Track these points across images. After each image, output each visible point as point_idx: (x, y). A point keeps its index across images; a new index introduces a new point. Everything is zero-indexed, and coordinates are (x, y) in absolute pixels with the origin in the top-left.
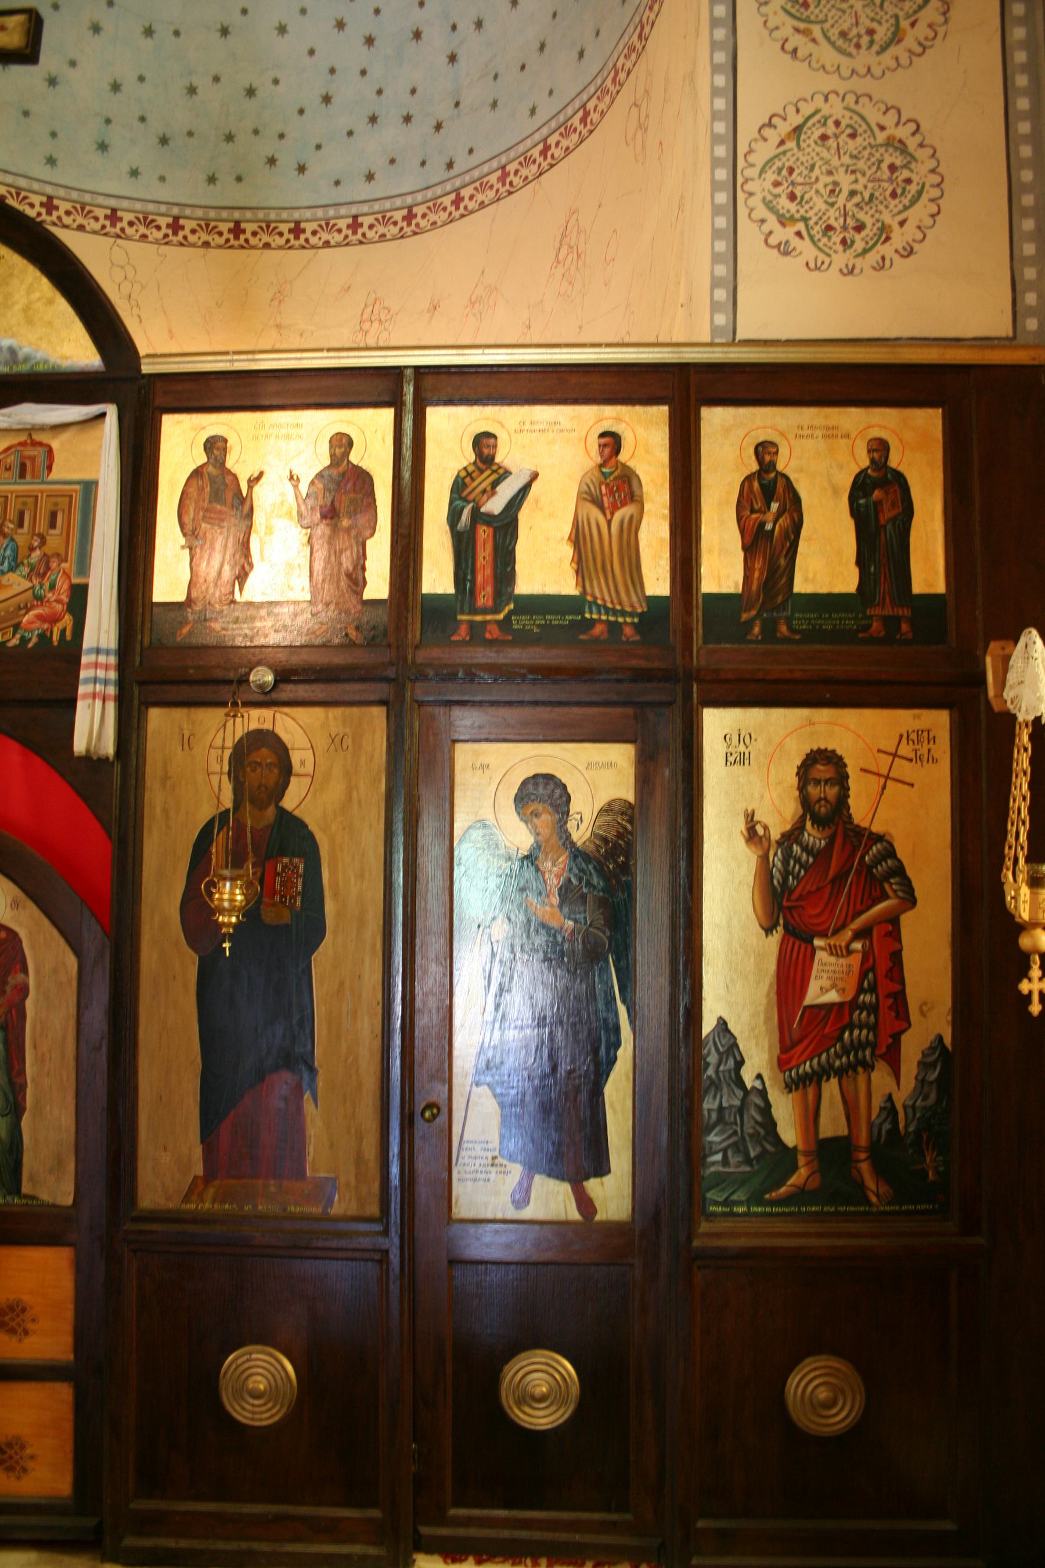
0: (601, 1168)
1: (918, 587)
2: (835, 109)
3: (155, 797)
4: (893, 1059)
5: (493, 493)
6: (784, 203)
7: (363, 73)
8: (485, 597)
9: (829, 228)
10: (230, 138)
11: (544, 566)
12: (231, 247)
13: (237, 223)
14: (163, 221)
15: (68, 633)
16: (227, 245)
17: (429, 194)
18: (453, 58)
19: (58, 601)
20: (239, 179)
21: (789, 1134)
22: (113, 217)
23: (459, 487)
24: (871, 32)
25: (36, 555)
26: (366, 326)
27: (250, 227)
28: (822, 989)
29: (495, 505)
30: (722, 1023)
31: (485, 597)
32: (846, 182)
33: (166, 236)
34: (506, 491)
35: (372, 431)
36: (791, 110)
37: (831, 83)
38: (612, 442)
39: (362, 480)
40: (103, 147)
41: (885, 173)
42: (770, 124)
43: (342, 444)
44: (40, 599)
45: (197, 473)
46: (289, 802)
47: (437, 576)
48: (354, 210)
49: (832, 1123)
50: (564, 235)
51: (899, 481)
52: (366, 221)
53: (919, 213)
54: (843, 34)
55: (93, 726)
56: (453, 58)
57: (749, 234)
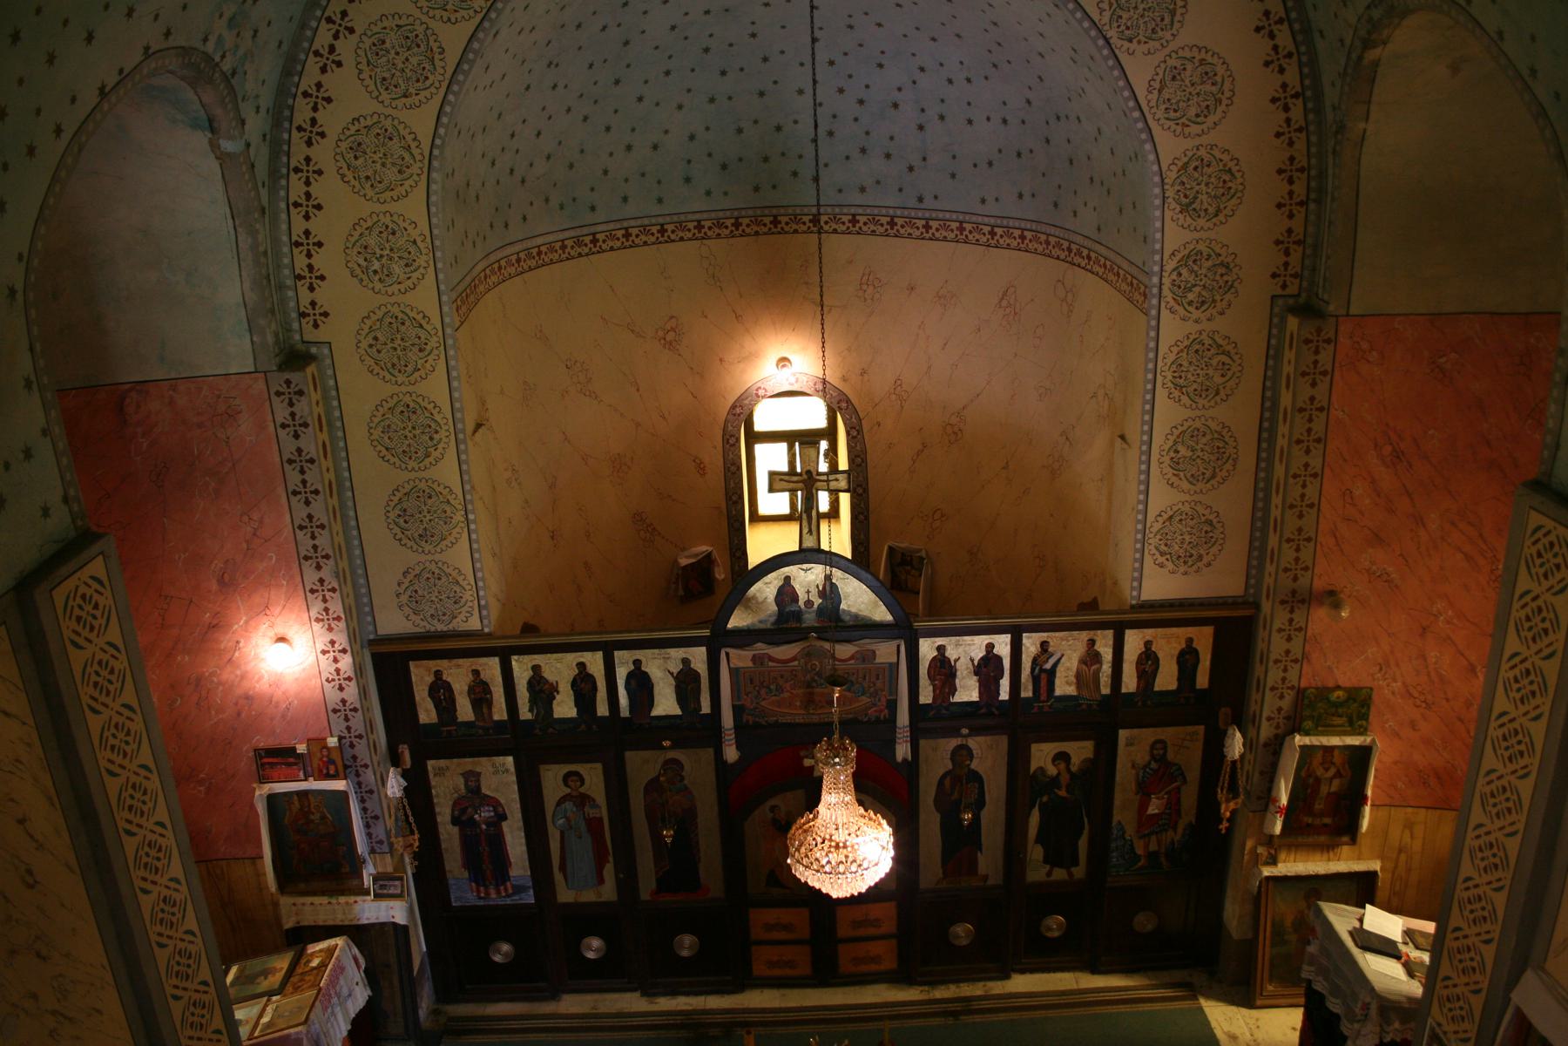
0: (1077, 864)
1: (1198, 687)
2: (1186, 508)
3: (923, 768)
4: (1175, 828)
6: (1163, 548)
7: (856, 119)
10: (766, 159)
11: (1064, 686)
14: (729, 222)
17: (906, 213)
18: (921, 128)
20: (774, 187)
21: (1140, 851)
22: (699, 227)
23: (1035, 661)
27: (784, 219)
28: (1152, 810)
29: (1048, 666)
32: (1187, 538)
34: (1052, 661)
37: (1187, 497)
38: (1092, 642)
39: (999, 659)
43: (990, 647)
47: (1027, 692)
48: (853, 211)
49: (1153, 847)
50: (1005, 294)
52: (862, 219)
53: (1214, 550)
55: (902, 751)
56: (921, 128)
57: (1148, 559)
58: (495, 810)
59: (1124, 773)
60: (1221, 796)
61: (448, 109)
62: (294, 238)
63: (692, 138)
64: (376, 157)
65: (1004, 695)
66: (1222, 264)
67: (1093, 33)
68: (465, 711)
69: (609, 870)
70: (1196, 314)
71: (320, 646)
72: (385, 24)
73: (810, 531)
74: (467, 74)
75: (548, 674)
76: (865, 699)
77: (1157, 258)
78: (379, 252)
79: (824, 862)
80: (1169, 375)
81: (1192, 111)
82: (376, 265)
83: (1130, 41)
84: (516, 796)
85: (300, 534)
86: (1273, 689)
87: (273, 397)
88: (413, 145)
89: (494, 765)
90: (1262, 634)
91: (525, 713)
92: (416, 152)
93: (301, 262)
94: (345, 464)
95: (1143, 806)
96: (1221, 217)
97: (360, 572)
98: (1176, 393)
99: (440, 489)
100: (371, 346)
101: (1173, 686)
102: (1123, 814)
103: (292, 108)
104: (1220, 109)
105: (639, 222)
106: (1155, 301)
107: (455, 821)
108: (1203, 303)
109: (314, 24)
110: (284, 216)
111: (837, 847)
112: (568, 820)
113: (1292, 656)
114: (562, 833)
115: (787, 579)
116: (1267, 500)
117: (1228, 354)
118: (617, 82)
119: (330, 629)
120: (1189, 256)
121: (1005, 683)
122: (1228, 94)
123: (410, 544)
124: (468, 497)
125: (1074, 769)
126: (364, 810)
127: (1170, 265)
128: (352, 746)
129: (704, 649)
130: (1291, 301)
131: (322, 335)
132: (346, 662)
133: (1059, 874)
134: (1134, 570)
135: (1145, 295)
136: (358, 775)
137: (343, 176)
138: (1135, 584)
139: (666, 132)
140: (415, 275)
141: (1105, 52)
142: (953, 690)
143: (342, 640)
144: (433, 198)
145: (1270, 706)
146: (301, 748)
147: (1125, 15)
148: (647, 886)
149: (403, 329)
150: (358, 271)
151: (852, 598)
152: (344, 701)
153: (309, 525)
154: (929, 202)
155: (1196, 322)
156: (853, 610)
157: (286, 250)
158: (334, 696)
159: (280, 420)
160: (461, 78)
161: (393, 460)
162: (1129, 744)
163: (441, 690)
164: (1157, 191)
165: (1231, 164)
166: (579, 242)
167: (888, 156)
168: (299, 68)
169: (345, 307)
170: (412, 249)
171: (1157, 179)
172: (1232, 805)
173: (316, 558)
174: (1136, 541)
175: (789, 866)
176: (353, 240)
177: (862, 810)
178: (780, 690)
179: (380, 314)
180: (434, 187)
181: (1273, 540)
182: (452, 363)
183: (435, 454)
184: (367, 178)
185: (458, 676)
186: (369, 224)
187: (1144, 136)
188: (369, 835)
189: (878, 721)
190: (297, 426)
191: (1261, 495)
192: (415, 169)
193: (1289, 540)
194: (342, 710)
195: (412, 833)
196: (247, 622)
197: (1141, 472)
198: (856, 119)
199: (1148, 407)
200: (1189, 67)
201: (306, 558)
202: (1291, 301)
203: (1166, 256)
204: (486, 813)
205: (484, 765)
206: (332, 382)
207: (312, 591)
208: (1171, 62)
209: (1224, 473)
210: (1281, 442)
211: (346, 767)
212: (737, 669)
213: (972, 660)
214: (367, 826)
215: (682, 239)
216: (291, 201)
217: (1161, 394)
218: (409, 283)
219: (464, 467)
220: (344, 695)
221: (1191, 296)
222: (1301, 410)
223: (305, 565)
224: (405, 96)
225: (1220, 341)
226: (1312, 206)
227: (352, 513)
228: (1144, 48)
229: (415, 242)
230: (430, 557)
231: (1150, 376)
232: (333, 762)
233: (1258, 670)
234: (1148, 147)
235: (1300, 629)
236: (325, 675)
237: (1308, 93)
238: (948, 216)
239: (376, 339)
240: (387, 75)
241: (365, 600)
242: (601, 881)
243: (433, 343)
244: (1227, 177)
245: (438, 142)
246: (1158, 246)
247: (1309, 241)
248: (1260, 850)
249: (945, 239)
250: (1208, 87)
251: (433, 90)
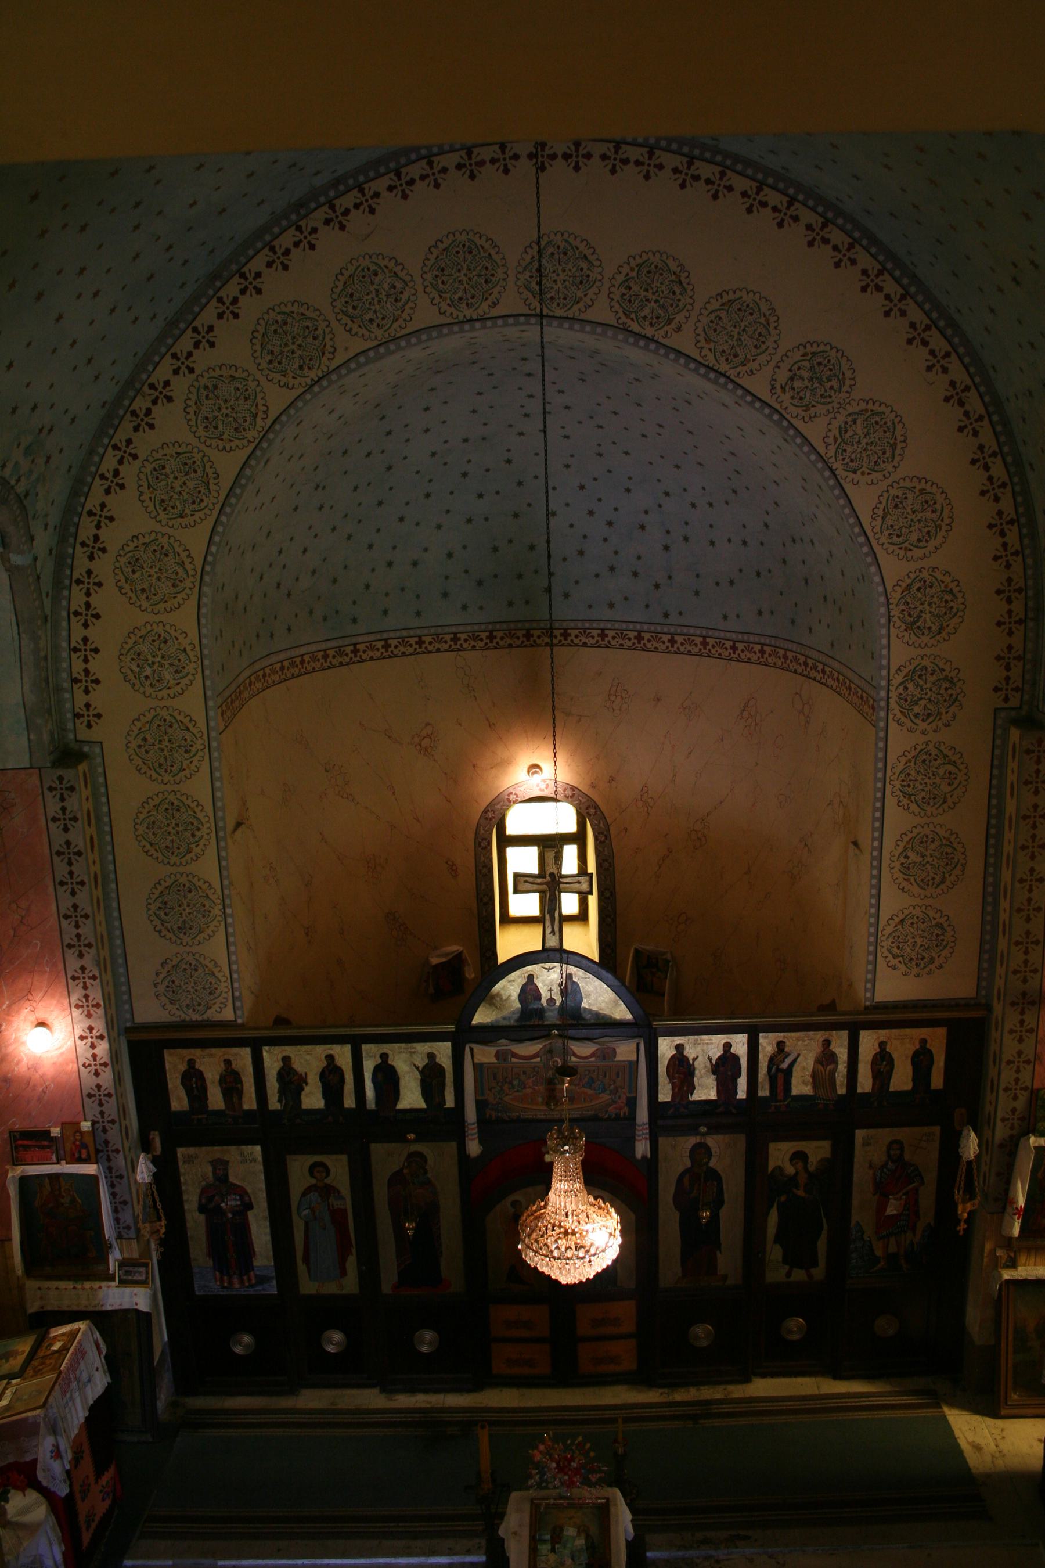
0: (815, 1264)
2: (917, 912)
5: (783, 1061)
6: (895, 950)
7: (605, 540)
8: (780, 1096)
9: (912, 959)
10: (520, 576)
11: (801, 1086)
12: (526, 646)
13: (528, 630)
14: (484, 635)
16: (522, 645)
17: (652, 628)
20: (527, 602)
21: (879, 1253)
23: (771, 1060)
24: (933, 879)
25: (612, 1087)
26: (613, 698)
28: (891, 1211)
30: (858, 1223)
31: (780, 1096)
32: (919, 941)
33: (486, 644)
34: (788, 1061)
35: (740, 1044)
36: (900, 913)
38: (827, 1043)
39: (736, 1058)
40: (445, 595)
41: (934, 937)
42: (892, 919)
43: (727, 1046)
45: (673, 1057)
46: (711, 1165)
47: (764, 1092)
48: (602, 625)
49: (892, 1249)
51: (930, 1052)
54: (922, 880)
55: (642, 1148)
56: (666, 548)
58: (242, 1199)
59: (861, 1176)
60: (958, 1196)
61: (220, 529)
62: (73, 644)
63: (450, 555)
64: (152, 572)
65: (742, 1094)
66: (946, 678)
67: (820, 465)
68: (216, 1099)
69: (351, 1262)
70: (923, 726)
71: (78, 1032)
72: (166, 451)
73: (553, 932)
74: (239, 498)
75: (297, 1065)
77: (884, 673)
78: (150, 657)
79: (553, 1247)
80: (898, 784)
81: (914, 537)
82: (148, 671)
83: (855, 472)
84: (263, 1186)
85: (65, 923)
86: (1006, 1089)
87: (46, 791)
88: (187, 561)
89: (242, 1154)
90: (995, 1035)
91: (274, 1103)
92: (188, 567)
93: (78, 666)
94: (110, 858)
95: (882, 1207)
96: (944, 634)
97: (121, 961)
98: (905, 801)
99: (201, 883)
100: (140, 746)
101: (908, 1086)
102: (861, 1214)
103: (77, 526)
104: (940, 534)
105: (398, 634)
106: (882, 714)
107: (202, 1209)
108: (929, 715)
109: (101, 450)
110: (64, 624)
111: (566, 1233)
112: (313, 1210)
113: (1023, 1057)
114: (307, 1224)
115: (531, 977)
116: (996, 904)
117: (954, 764)
118: (380, 503)
119: (89, 1015)
120: (914, 671)
121: (742, 1083)
122: (947, 521)
123: (169, 935)
124: (226, 892)
125: (812, 1168)
126: (113, 1195)
127: (897, 680)
128: (105, 1130)
129: (449, 1044)
130: (1013, 713)
131: (94, 735)
132: (103, 1048)
133: (799, 1275)
134: (868, 972)
135: (873, 708)
136: (109, 1160)
137: (121, 588)
138: (869, 986)
139: (426, 550)
140: (184, 681)
141: (832, 482)
142: (692, 1088)
143: (100, 1027)
144: (203, 611)
145: (1004, 1106)
146: (55, 1132)
147: (849, 449)
148: (389, 1278)
149: (170, 731)
150: (131, 676)
151: (593, 997)
152: (99, 1087)
153: (74, 915)
154: (673, 619)
155: (923, 733)
156: (594, 1008)
157: (65, 655)
158: (89, 1081)
159: (50, 815)
160: (233, 500)
161: (156, 854)
162: (866, 1143)
163: (193, 1079)
164: (883, 610)
165: (953, 585)
166: (340, 652)
167: (635, 574)
168: (86, 489)
169: (117, 709)
170: (182, 657)
171: (882, 599)
172: (969, 1206)
173: (78, 946)
174: (869, 944)
175: (519, 1252)
176: (127, 647)
177: (592, 1199)
179: (149, 717)
180: (204, 600)
181: (1002, 944)
182: (216, 764)
183: (197, 850)
184: (143, 590)
185: (211, 1065)
186: (143, 632)
187: (869, 559)
188: (117, 1220)
189: (618, 1118)
190: (66, 820)
191: (990, 899)
192: (188, 583)
193: (1017, 943)
194: (98, 1095)
195: (160, 1220)
196: (9, 1006)
197: (872, 877)
198: (605, 540)
199: (878, 814)
200: (910, 496)
201: (70, 946)
202: (1013, 713)
203: (893, 671)
204: (232, 1202)
205: (232, 1154)
206: (101, 780)
207: (74, 978)
208: (893, 492)
209: (953, 878)
210: (1008, 848)
211: (97, 1151)
212: (481, 1065)
213: (710, 1059)
214: (116, 1211)
215: (438, 650)
216: (72, 609)
217: (890, 802)
218: (178, 689)
219: (224, 863)
220: (99, 1080)
221: (917, 709)
222: (1025, 817)
223: (69, 952)
224: (181, 516)
225: (946, 752)
226: (1031, 624)
227: (115, 904)
228: (868, 479)
229: (185, 650)
230: (187, 949)
231: (879, 785)
232: (86, 1147)
233: (992, 1072)
234: (873, 569)
235: (1031, 1031)
236: (82, 1061)
237: (1023, 520)
238: (692, 631)
239: (145, 739)
240: (165, 497)
241: (124, 988)
242: (343, 1273)
243: (198, 745)
244: (948, 597)
245: (210, 558)
246: (884, 662)
247: (1029, 656)
248: (999, 1252)
249: (689, 653)
250: (928, 514)
251: (206, 511)
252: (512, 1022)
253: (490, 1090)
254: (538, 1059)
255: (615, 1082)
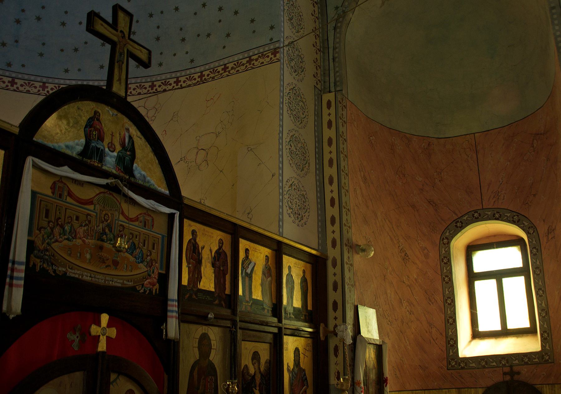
15: (158, 290)
19: (155, 278)
25: (149, 258)
31: (247, 299)
32: (298, 201)
44: (149, 275)
55: (172, 328)
76: (143, 268)
142: (199, 278)
178: (74, 234)
213: (211, 251)
252: (74, 155)
253: (39, 229)
254: (91, 207)
255: (151, 254)
